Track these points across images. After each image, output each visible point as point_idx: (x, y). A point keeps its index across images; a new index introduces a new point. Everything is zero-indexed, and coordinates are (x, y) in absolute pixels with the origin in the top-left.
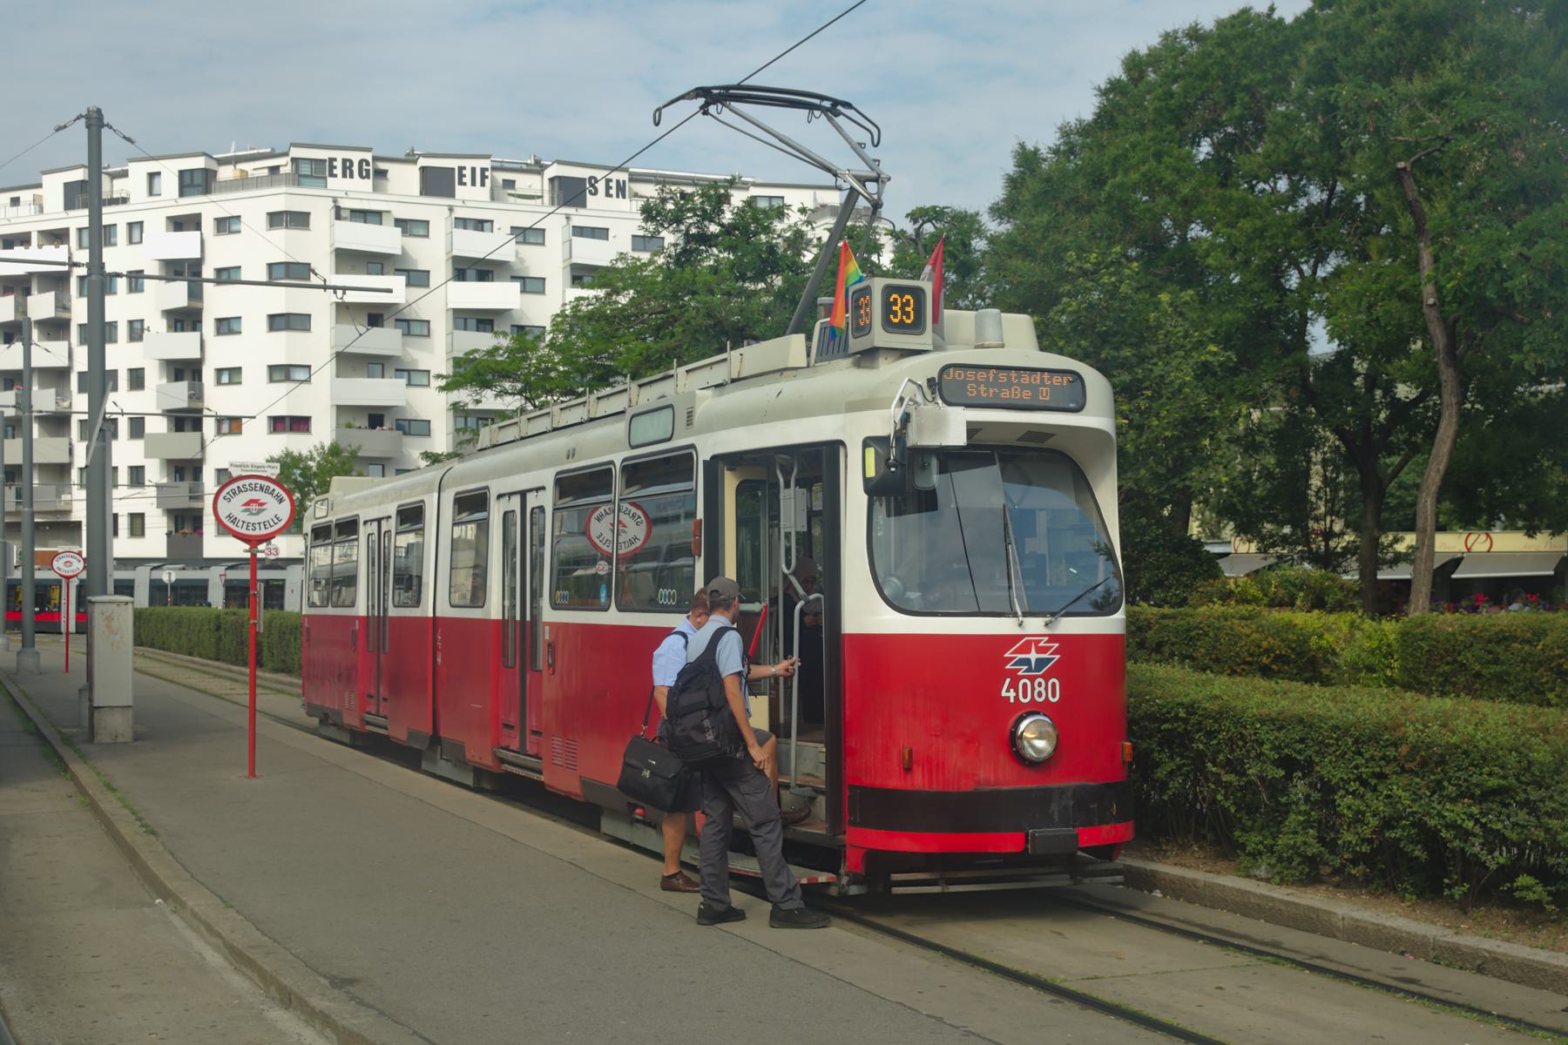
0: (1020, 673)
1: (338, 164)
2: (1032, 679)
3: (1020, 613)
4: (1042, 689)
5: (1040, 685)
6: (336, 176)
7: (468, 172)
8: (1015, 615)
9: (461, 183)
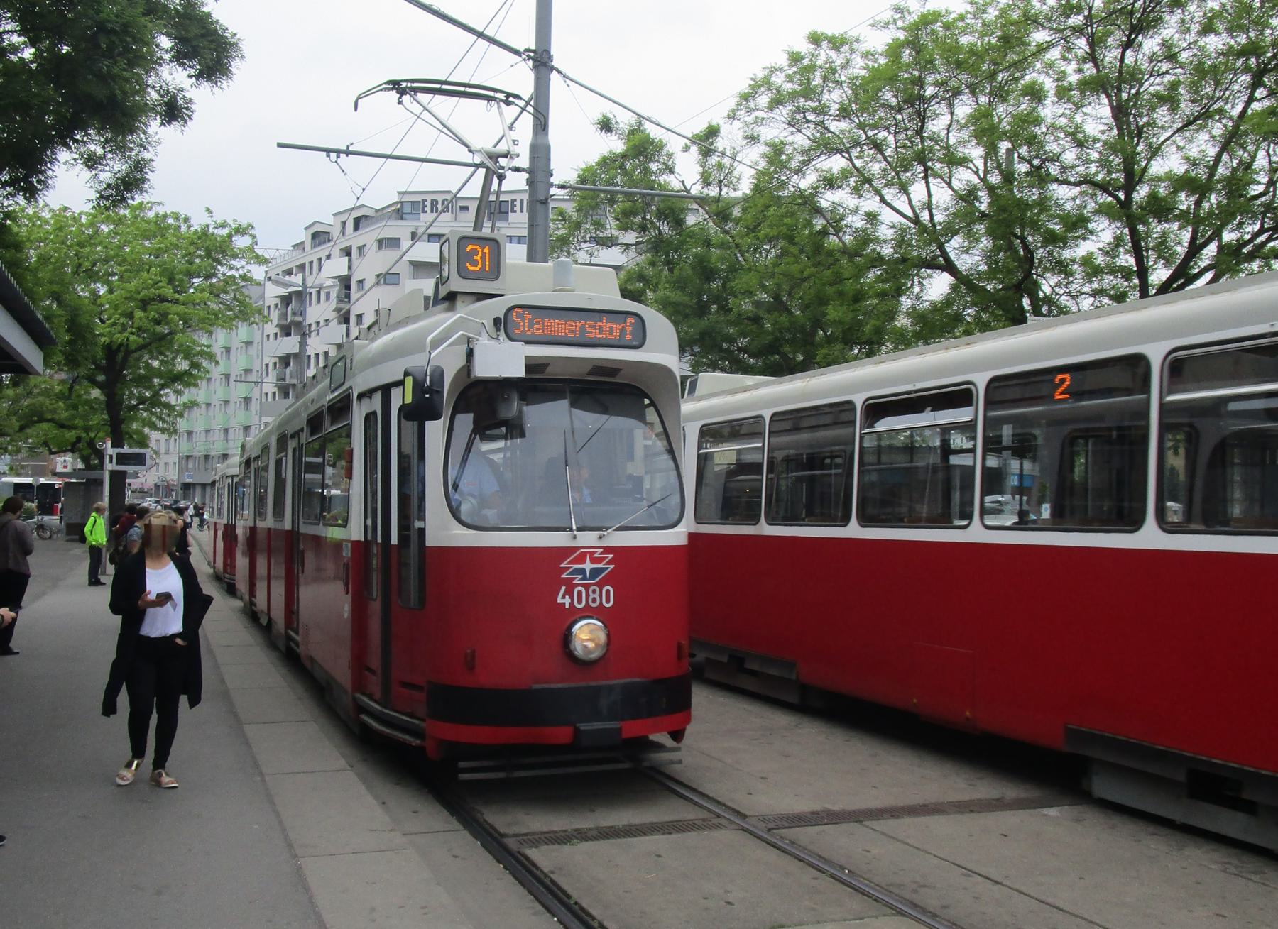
0: (575, 582)
1: (428, 204)
2: (587, 587)
3: (574, 527)
4: (597, 596)
5: (594, 591)
6: (426, 212)
7: (518, 203)
8: (571, 530)
9: (513, 211)
